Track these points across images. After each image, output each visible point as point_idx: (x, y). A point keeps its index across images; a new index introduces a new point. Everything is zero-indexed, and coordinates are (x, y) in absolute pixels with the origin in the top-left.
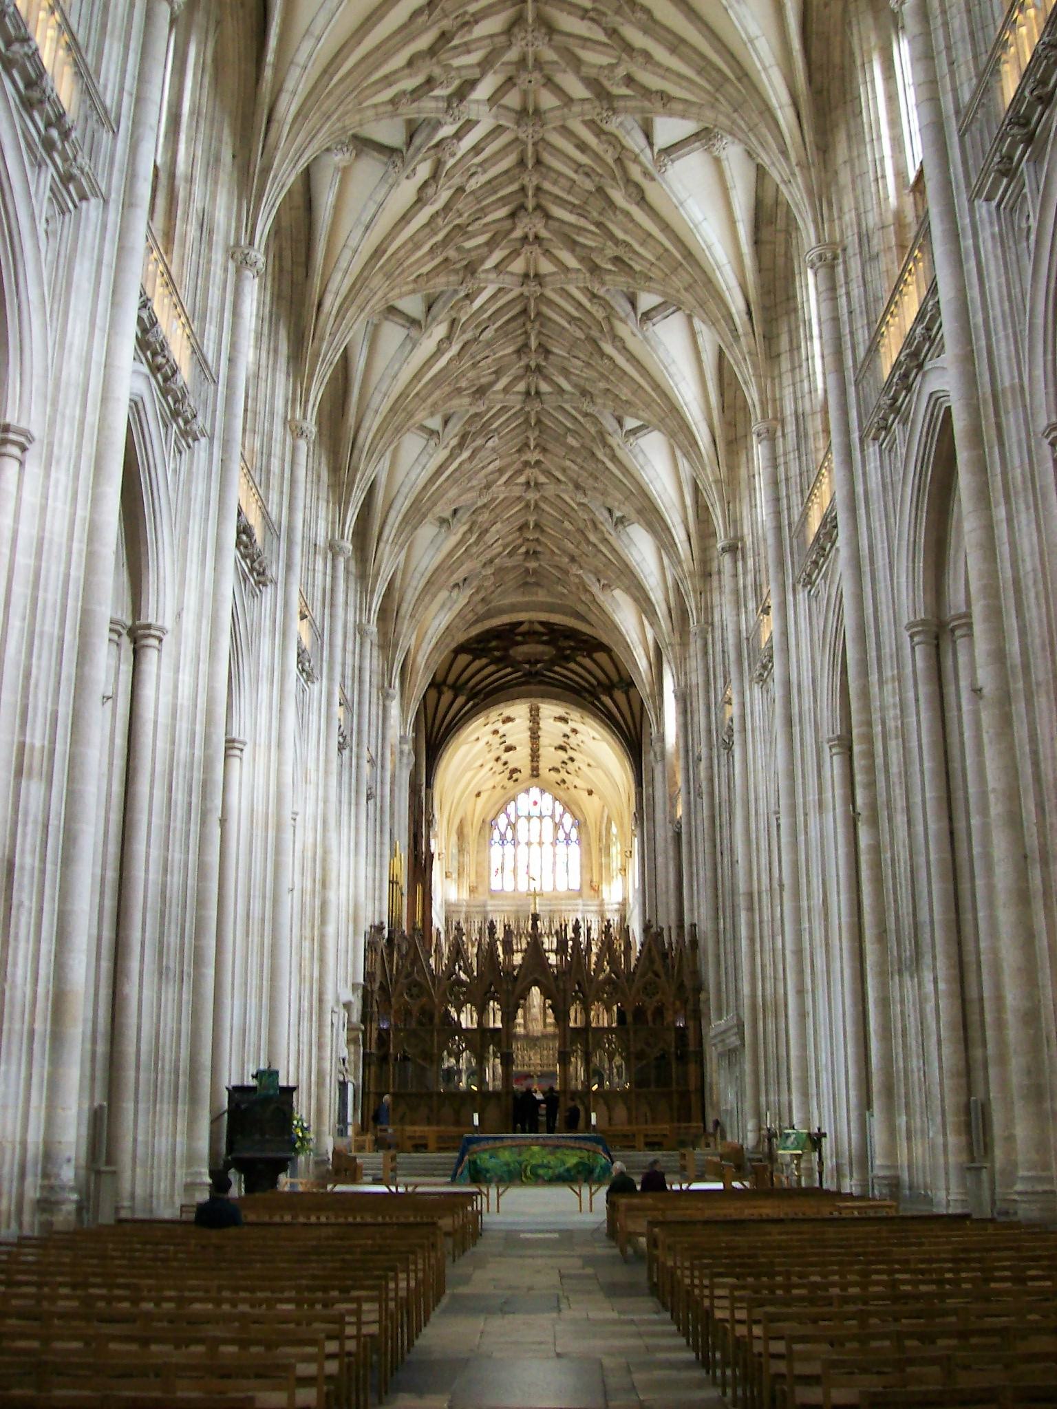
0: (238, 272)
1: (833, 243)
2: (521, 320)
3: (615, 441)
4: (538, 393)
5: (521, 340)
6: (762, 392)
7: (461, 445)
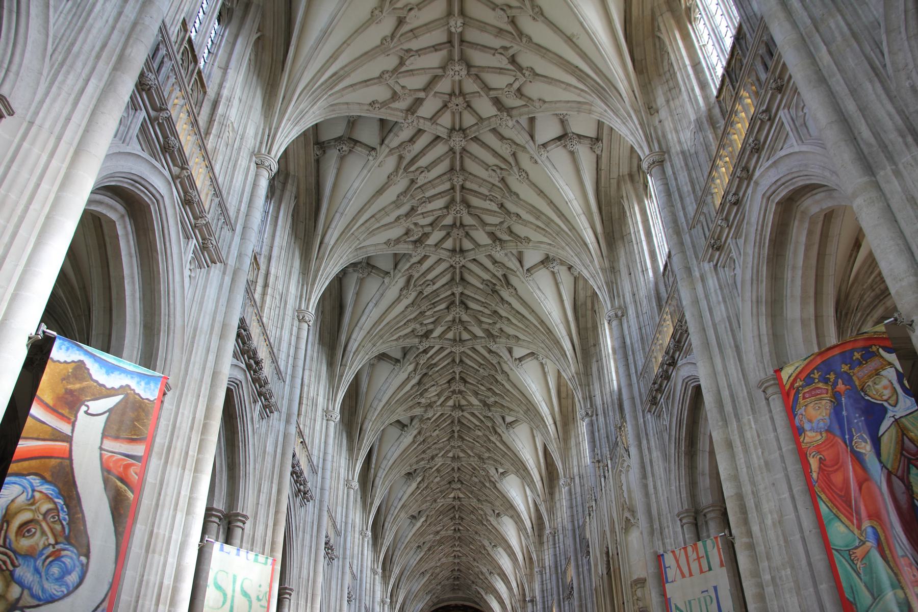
0: (363, 539)
1: (554, 528)
2: (452, 510)
3: (489, 549)
4: (459, 529)
5: (452, 515)
6: (537, 555)
7: (429, 550)
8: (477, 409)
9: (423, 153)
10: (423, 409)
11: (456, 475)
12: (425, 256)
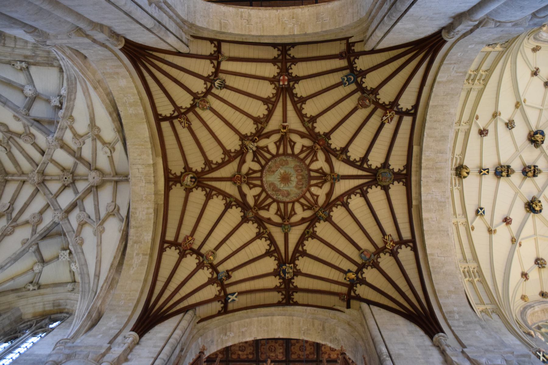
9: (23, 151)
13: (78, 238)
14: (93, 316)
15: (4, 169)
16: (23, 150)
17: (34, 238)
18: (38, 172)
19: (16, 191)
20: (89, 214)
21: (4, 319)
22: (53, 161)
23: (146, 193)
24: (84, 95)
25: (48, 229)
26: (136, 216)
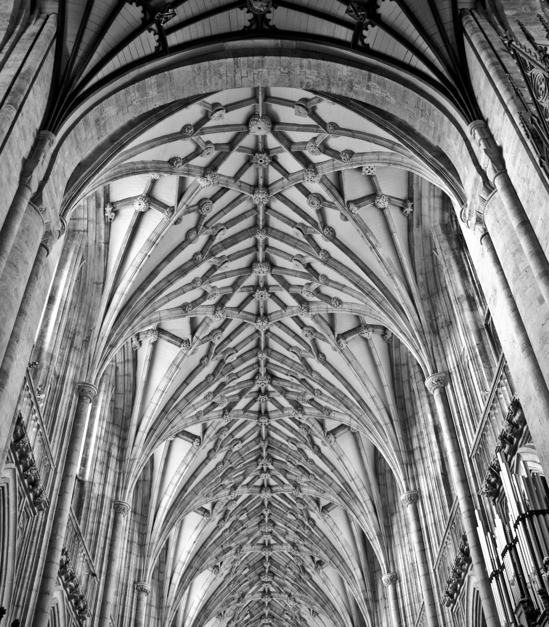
8: (288, 491)
9: (223, 211)
10: (228, 492)
11: (267, 565)
12: (227, 319)
13: (343, 158)
14: (443, 166)
15: (250, 228)
16: (222, 210)
17: (340, 207)
18: (253, 193)
19: (278, 218)
20: (311, 138)
21: (441, 248)
22: (237, 177)
23: (279, 68)
24: (134, 156)
25: (329, 189)
26: (312, 83)
